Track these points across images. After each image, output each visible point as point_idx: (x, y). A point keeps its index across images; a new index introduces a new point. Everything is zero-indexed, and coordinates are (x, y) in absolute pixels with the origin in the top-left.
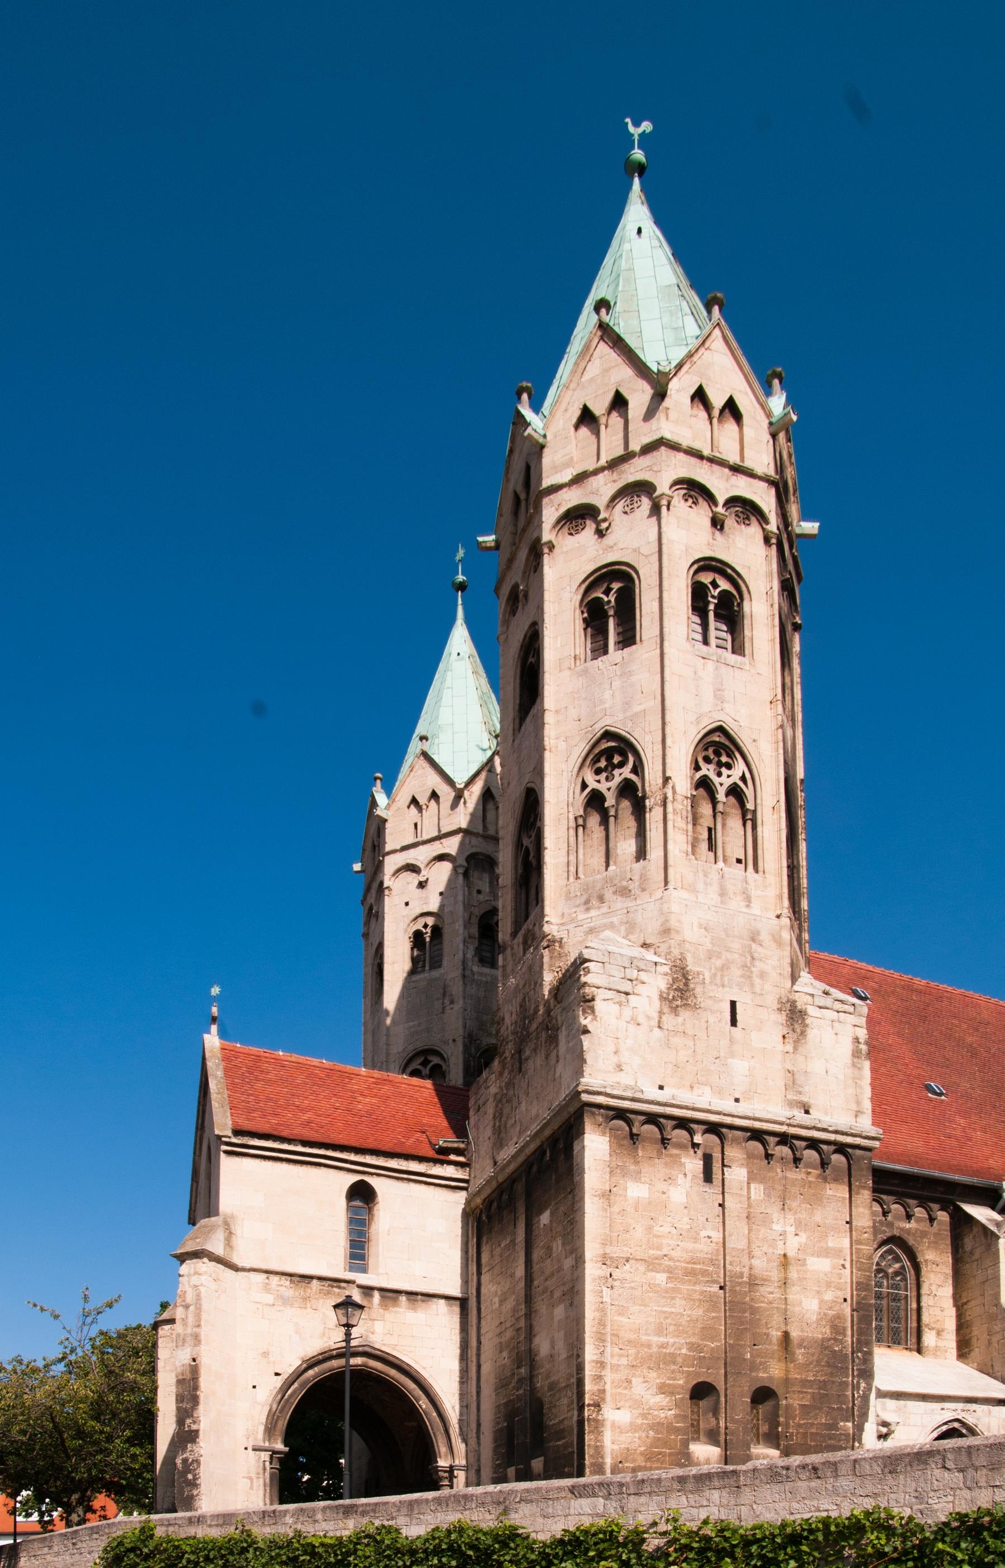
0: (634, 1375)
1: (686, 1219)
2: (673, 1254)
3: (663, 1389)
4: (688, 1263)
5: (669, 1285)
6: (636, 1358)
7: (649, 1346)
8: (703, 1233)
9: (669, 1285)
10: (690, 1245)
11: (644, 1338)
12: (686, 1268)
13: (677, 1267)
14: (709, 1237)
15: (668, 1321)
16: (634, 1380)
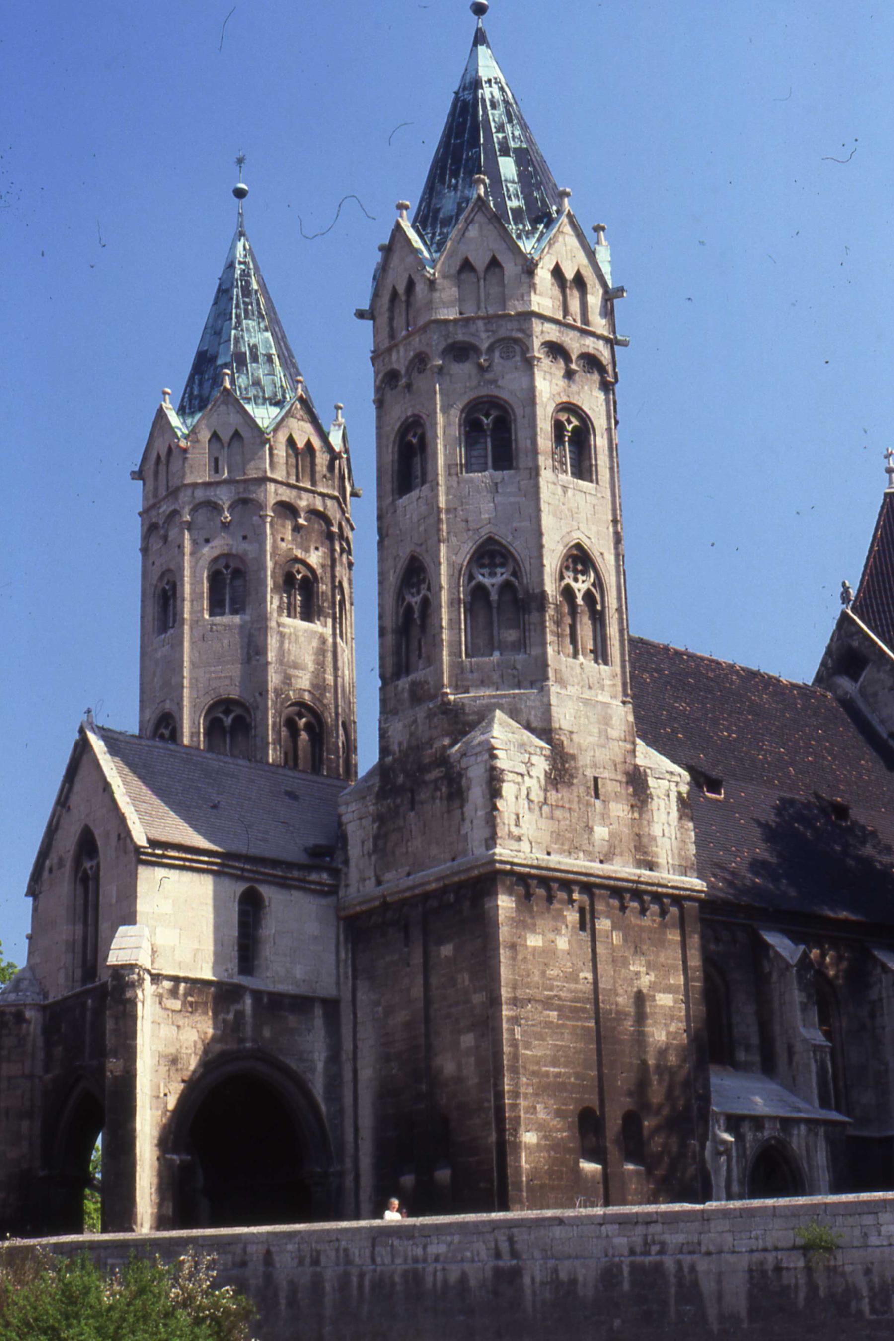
0: (538, 1103)
1: (569, 964)
2: (562, 994)
3: (559, 1113)
4: (572, 1002)
5: (560, 1022)
6: (538, 1088)
7: (547, 1074)
8: (582, 975)
9: (560, 1022)
10: (573, 986)
11: (544, 1069)
12: (571, 1006)
13: (564, 1006)
14: (586, 979)
15: (560, 1053)
16: (538, 1106)
